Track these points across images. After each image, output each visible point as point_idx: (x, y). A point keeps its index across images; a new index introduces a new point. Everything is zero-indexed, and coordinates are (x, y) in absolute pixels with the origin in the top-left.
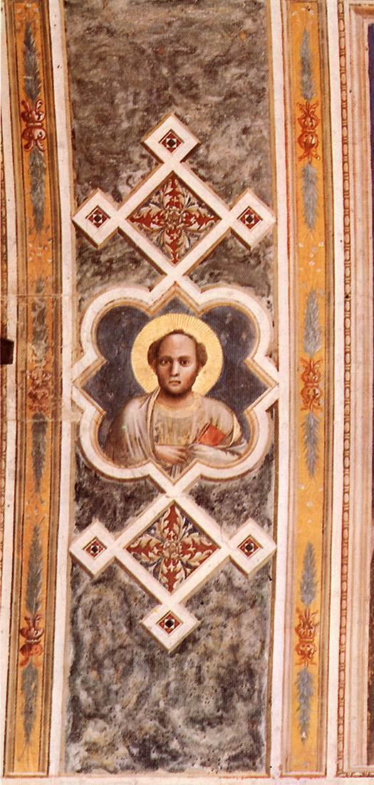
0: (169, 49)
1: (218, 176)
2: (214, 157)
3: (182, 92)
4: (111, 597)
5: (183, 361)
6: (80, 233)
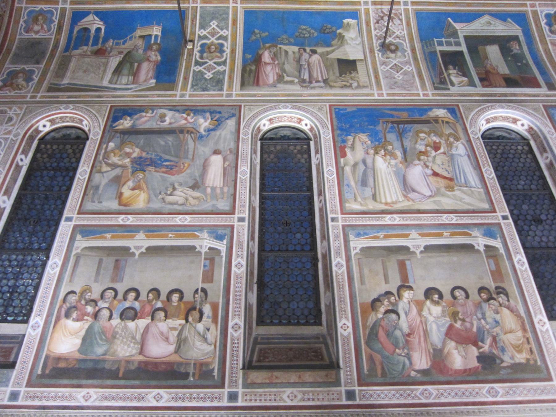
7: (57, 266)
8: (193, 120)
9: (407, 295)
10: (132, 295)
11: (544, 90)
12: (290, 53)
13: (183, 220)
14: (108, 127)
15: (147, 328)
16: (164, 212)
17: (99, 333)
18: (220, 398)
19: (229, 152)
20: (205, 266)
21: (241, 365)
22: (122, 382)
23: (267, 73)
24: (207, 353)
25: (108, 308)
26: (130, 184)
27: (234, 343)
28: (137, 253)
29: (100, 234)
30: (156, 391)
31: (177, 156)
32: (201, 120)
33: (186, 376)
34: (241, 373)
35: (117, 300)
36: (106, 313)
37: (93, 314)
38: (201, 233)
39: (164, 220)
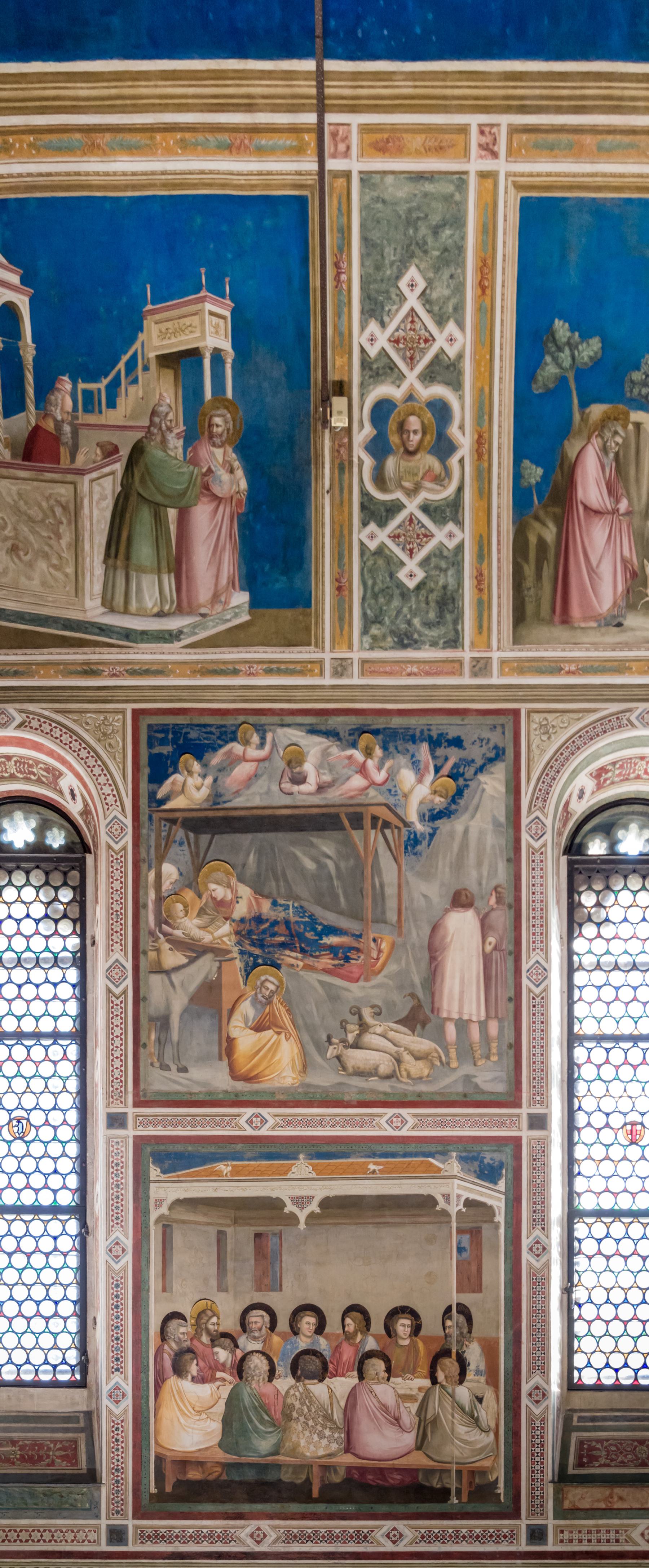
0: (414, 215)
1: (436, 309)
2: (434, 295)
3: (420, 248)
4: (381, 562)
5: (415, 432)
6: (363, 350)
7: (123, 1250)
10: (308, 1322)
13: (397, 1122)
14: (144, 801)
15: (353, 1395)
16: (347, 1098)
17: (255, 1408)
18: (512, 1536)
19: (493, 900)
20: (460, 1250)
22: (321, 1508)
23: (594, 562)
24: (482, 1450)
26: (246, 1008)
27: (533, 1428)
28: (302, 1216)
29: (204, 1164)
30: (388, 1525)
31: (355, 914)
33: (443, 1494)
34: (550, 1490)
35: (279, 1335)
36: (258, 1364)
37: (232, 1367)
38: (443, 1162)
39: (348, 1122)
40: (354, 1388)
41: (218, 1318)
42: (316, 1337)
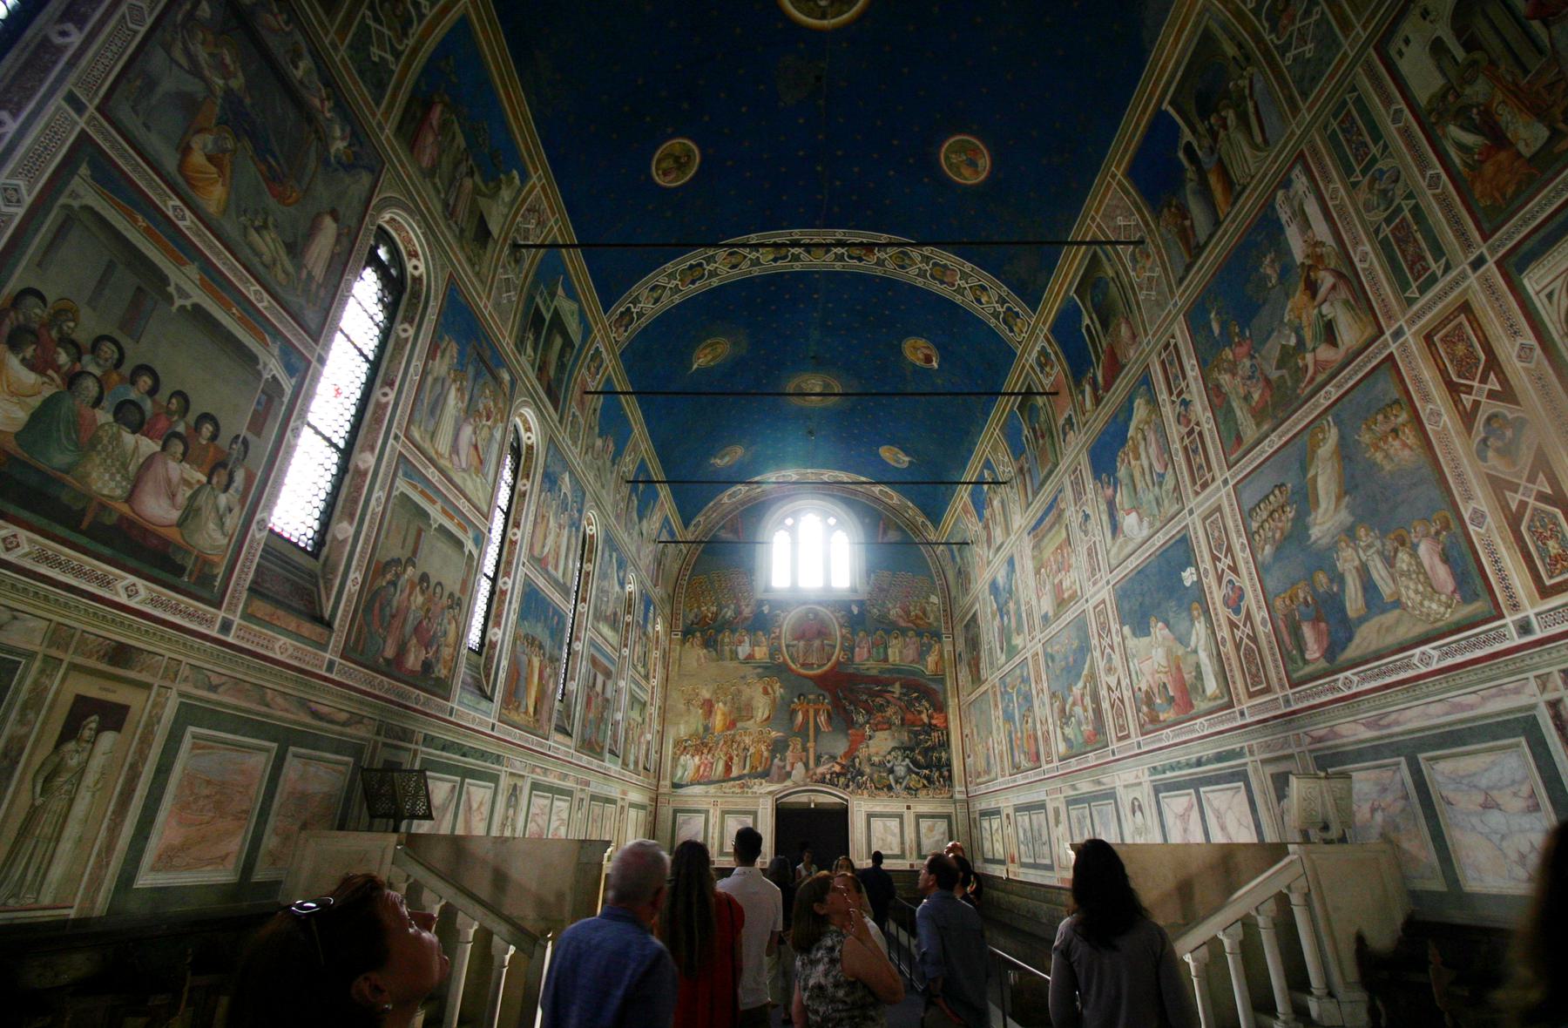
8: (328, 115)
9: (410, 570)
10: (145, 381)
11: (556, 417)
12: (455, 146)
15: (151, 459)
18: (209, 622)
20: (259, 403)
21: (247, 586)
24: (219, 547)
25: (99, 380)
28: (178, 302)
30: (132, 579)
32: (338, 133)
33: (179, 570)
34: (245, 595)
35: (119, 375)
39: (233, 269)
40: (154, 454)
41: (76, 325)
42: (146, 396)
